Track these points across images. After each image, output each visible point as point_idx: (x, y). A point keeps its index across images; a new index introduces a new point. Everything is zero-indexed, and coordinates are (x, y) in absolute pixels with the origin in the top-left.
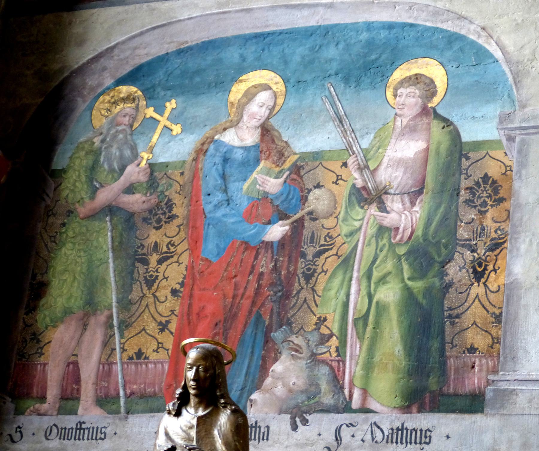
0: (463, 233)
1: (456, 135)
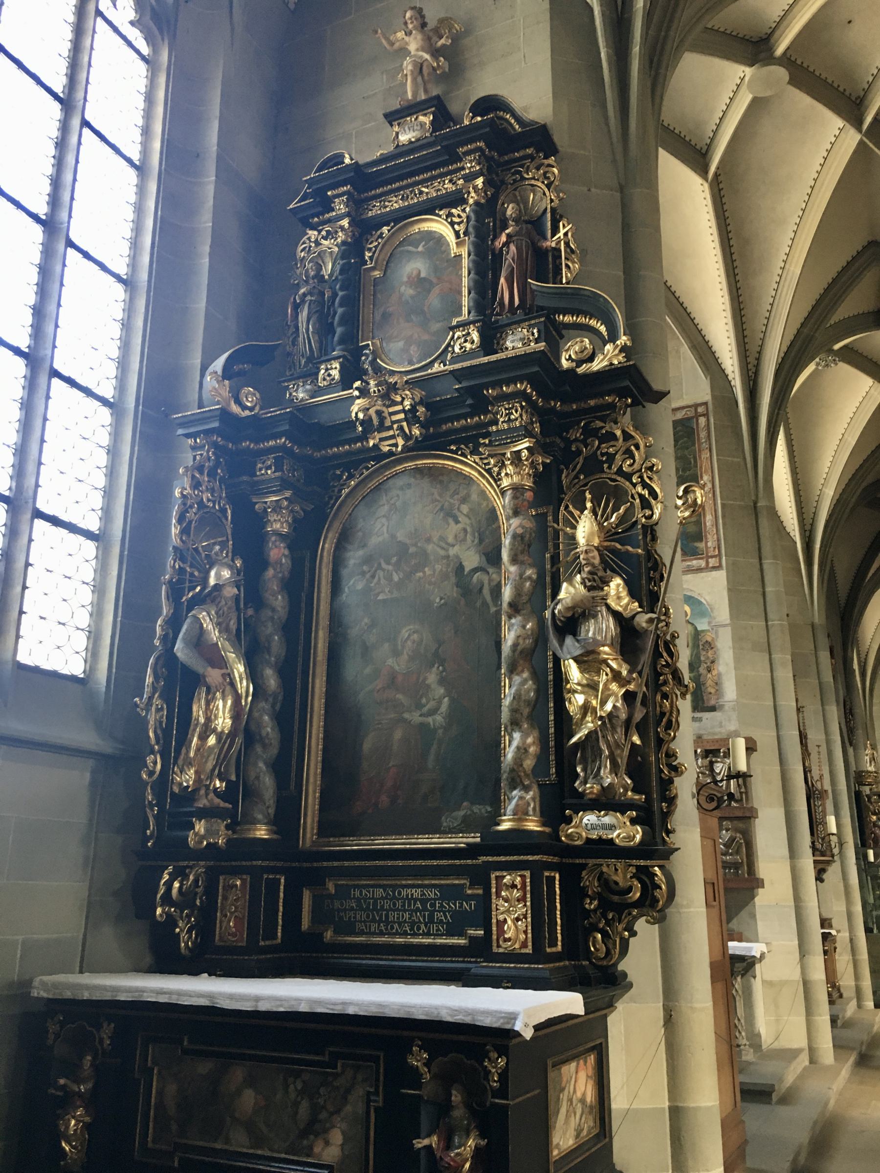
0: (702, 658)
1: (696, 628)
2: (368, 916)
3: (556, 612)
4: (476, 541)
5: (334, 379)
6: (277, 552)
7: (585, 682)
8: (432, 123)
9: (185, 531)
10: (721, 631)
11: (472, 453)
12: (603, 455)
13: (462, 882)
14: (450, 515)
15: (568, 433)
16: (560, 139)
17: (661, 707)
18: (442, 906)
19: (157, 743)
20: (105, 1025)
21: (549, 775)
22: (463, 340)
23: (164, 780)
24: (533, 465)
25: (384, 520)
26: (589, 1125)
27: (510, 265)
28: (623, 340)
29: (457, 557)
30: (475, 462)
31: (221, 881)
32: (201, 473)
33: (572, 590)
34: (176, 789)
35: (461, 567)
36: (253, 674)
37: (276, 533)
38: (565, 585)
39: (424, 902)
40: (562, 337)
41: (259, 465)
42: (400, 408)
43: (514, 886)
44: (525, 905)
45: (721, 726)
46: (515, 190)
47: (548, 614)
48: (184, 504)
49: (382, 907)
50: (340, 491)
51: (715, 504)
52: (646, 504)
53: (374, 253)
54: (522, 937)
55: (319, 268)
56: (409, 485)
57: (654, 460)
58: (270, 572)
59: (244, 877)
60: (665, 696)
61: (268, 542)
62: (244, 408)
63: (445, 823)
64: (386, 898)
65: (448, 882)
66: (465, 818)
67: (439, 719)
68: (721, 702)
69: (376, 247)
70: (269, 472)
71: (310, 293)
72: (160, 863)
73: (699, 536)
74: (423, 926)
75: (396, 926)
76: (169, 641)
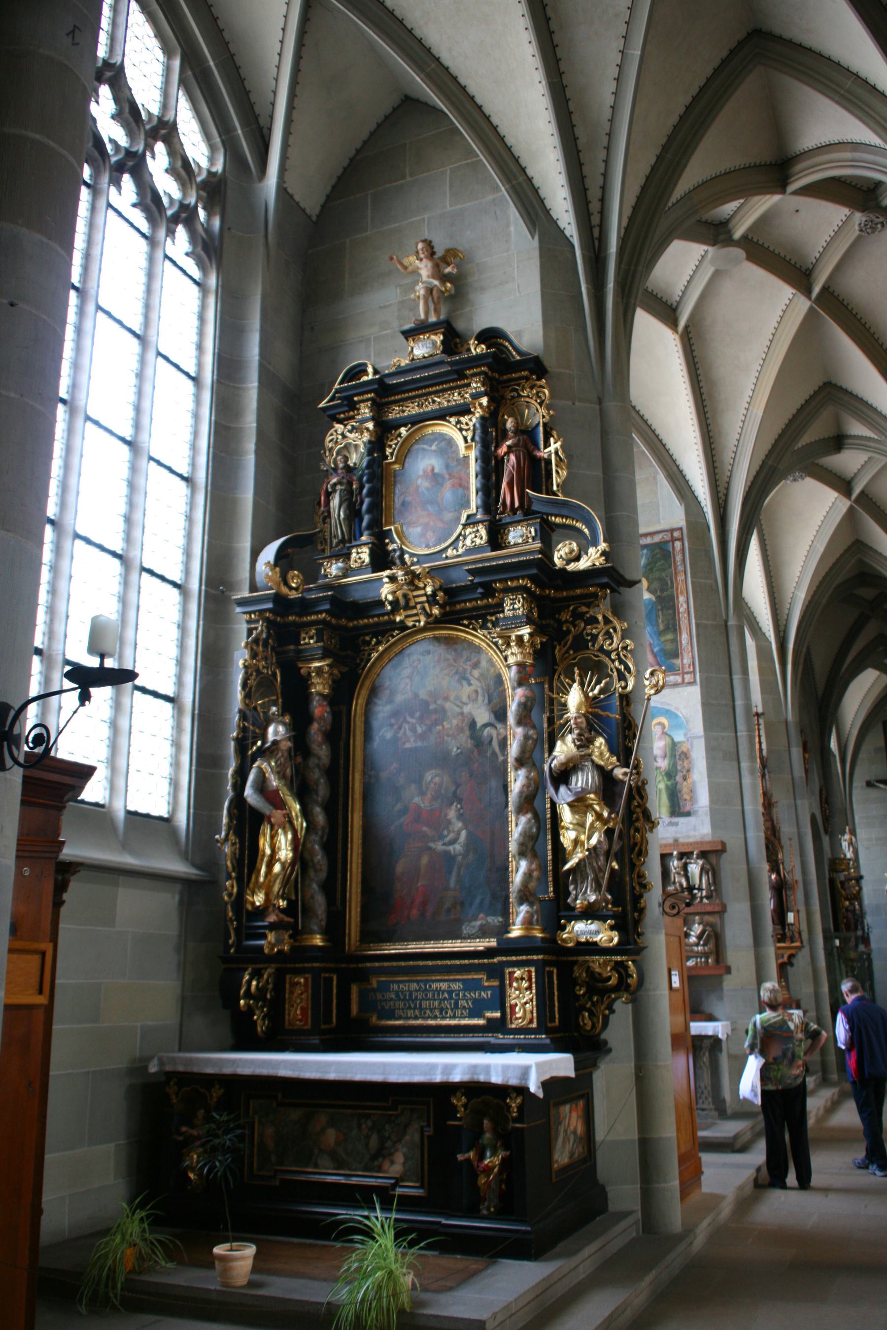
0: (679, 768)
1: (673, 740)
2: (405, 1005)
3: (553, 765)
4: (486, 701)
5: (363, 562)
6: (319, 709)
7: (575, 822)
8: (443, 342)
9: (248, 696)
10: (696, 742)
11: (482, 628)
12: (588, 635)
13: (480, 976)
14: (463, 678)
15: (559, 615)
16: (550, 363)
17: (634, 838)
18: (464, 995)
19: (234, 870)
20: (217, 1087)
21: (547, 892)
22: (473, 535)
23: (239, 901)
24: (533, 645)
25: (408, 680)
26: (579, 1151)
27: (510, 472)
28: (603, 546)
29: (470, 714)
30: (484, 635)
31: (288, 981)
32: (258, 645)
33: (565, 748)
34: (249, 907)
35: (473, 724)
36: (306, 813)
37: (320, 694)
38: (559, 743)
39: (450, 992)
40: (553, 531)
41: (303, 635)
42: (422, 592)
43: (522, 979)
44: (531, 993)
45: (695, 829)
46: (513, 404)
47: (546, 768)
48: (246, 673)
49: (416, 998)
50: (370, 655)
51: (690, 624)
52: (622, 677)
53: (394, 449)
54: (529, 1016)
55: (346, 459)
56: (428, 652)
57: (628, 642)
58: (315, 726)
59: (307, 976)
60: (637, 830)
61: (312, 701)
62: (291, 588)
63: (466, 930)
64: (419, 990)
65: (470, 977)
66: (481, 927)
67: (458, 848)
68: (696, 807)
69: (396, 444)
70: (312, 641)
71: (340, 483)
72: (241, 966)
73: (676, 654)
74: (449, 1011)
75: (428, 1012)
76: (239, 787)
